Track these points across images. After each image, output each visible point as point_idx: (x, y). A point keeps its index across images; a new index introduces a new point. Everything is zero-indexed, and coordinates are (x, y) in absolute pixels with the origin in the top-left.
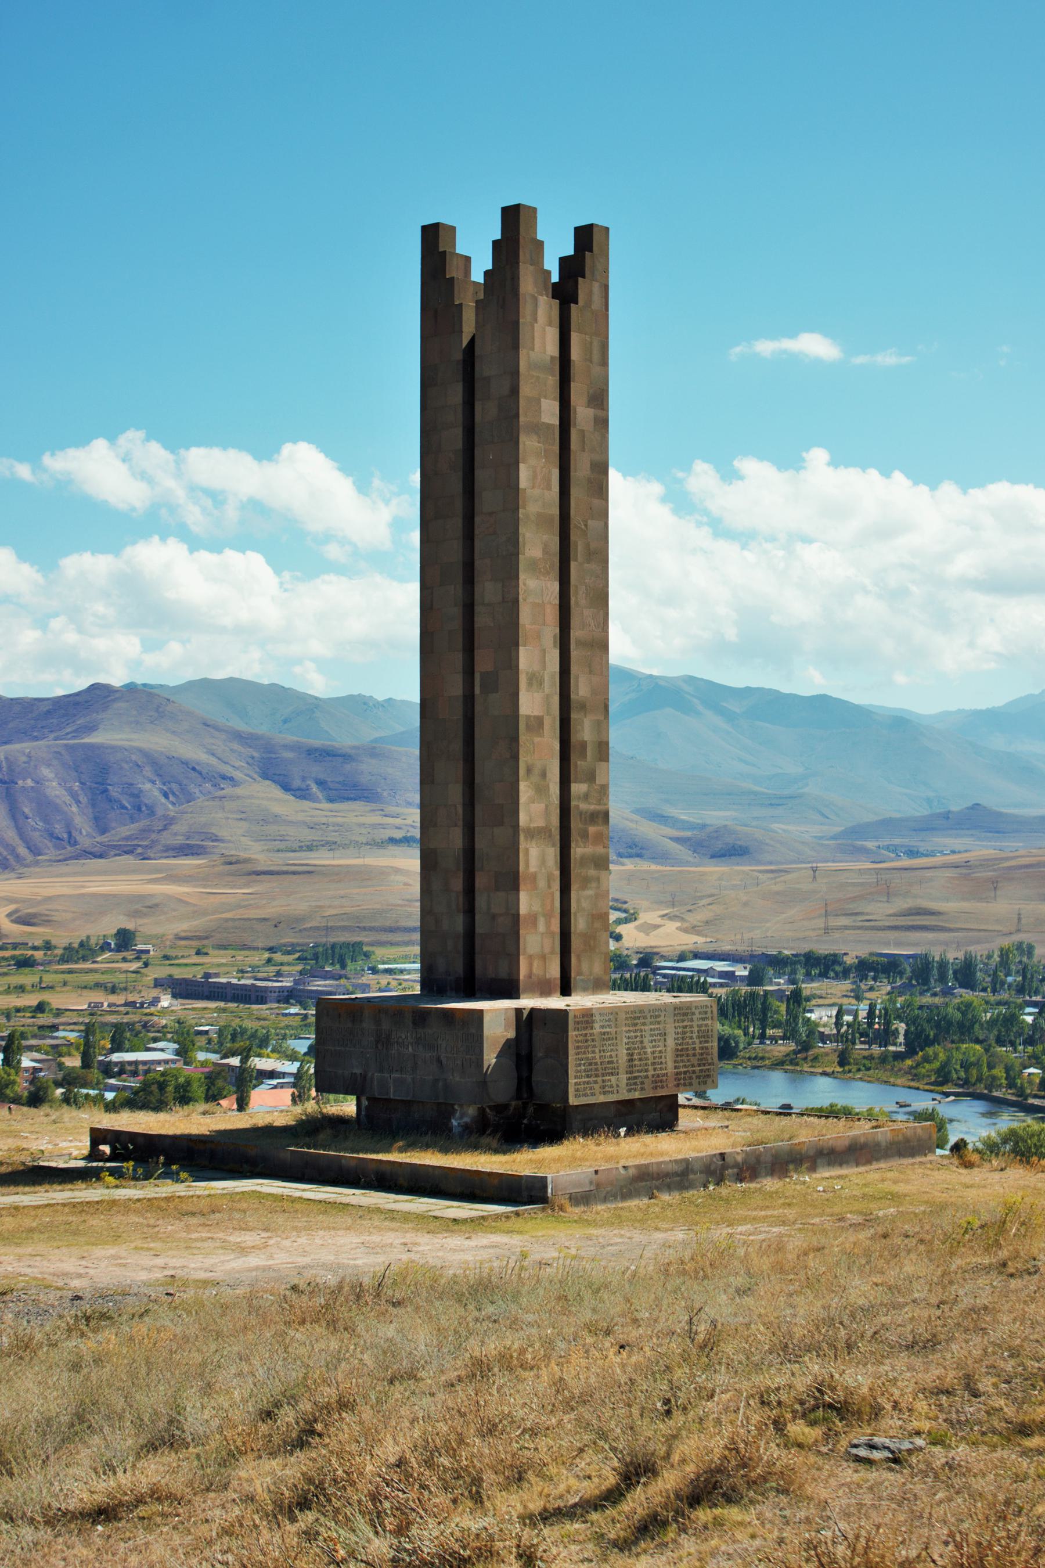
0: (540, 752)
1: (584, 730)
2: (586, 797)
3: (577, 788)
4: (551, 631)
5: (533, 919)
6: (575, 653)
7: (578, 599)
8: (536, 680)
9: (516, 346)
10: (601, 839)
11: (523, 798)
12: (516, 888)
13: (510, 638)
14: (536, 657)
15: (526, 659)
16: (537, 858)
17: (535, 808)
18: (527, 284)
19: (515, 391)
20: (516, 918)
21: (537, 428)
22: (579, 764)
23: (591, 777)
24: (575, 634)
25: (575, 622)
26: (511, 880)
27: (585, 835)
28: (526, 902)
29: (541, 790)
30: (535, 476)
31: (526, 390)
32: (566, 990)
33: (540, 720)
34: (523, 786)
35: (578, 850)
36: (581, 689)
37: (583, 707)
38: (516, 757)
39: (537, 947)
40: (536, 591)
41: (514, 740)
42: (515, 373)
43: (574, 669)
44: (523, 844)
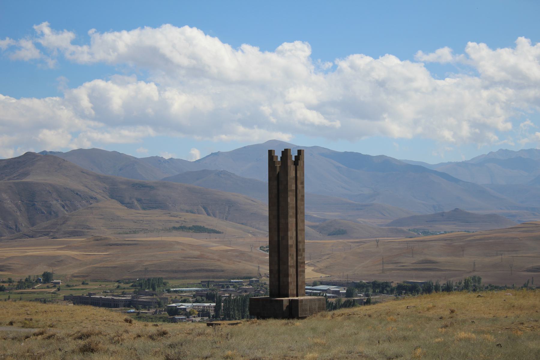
0: (292, 251)
1: (300, 247)
2: (301, 259)
3: (299, 258)
4: (294, 228)
5: (291, 283)
6: (298, 232)
7: (299, 221)
8: (291, 238)
9: (287, 175)
10: (304, 267)
11: (289, 260)
12: (288, 277)
13: (286, 230)
14: (291, 233)
15: (290, 234)
16: (292, 271)
17: (291, 262)
18: (290, 163)
19: (287, 184)
20: (288, 282)
21: (291, 190)
22: (299, 253)
23: (302, 255)
24: (299, 228)
25: (298, 226)
26: (287, 275)
27: (300, 266)
28: (290, 279)
29: (292, 258)
30: (291, 200)
31: (289, 184)
32: (297, 296)
33: (292, 245)
34: (289, 258)
35: (299, 269)
36: (300, 239)
37: (300, 242)
38: (288, 252)
39: (292, 288)
40: (291, 221)
41: (288, 249)
42: (287, 180)
43: (298, 235)
44: (289, 268)
